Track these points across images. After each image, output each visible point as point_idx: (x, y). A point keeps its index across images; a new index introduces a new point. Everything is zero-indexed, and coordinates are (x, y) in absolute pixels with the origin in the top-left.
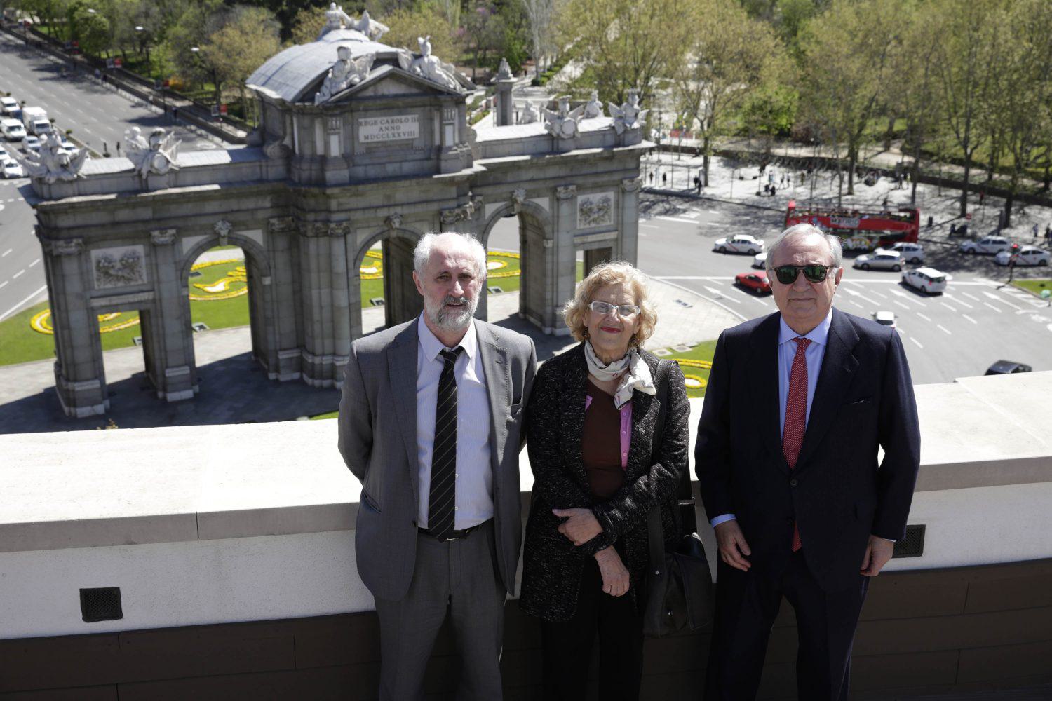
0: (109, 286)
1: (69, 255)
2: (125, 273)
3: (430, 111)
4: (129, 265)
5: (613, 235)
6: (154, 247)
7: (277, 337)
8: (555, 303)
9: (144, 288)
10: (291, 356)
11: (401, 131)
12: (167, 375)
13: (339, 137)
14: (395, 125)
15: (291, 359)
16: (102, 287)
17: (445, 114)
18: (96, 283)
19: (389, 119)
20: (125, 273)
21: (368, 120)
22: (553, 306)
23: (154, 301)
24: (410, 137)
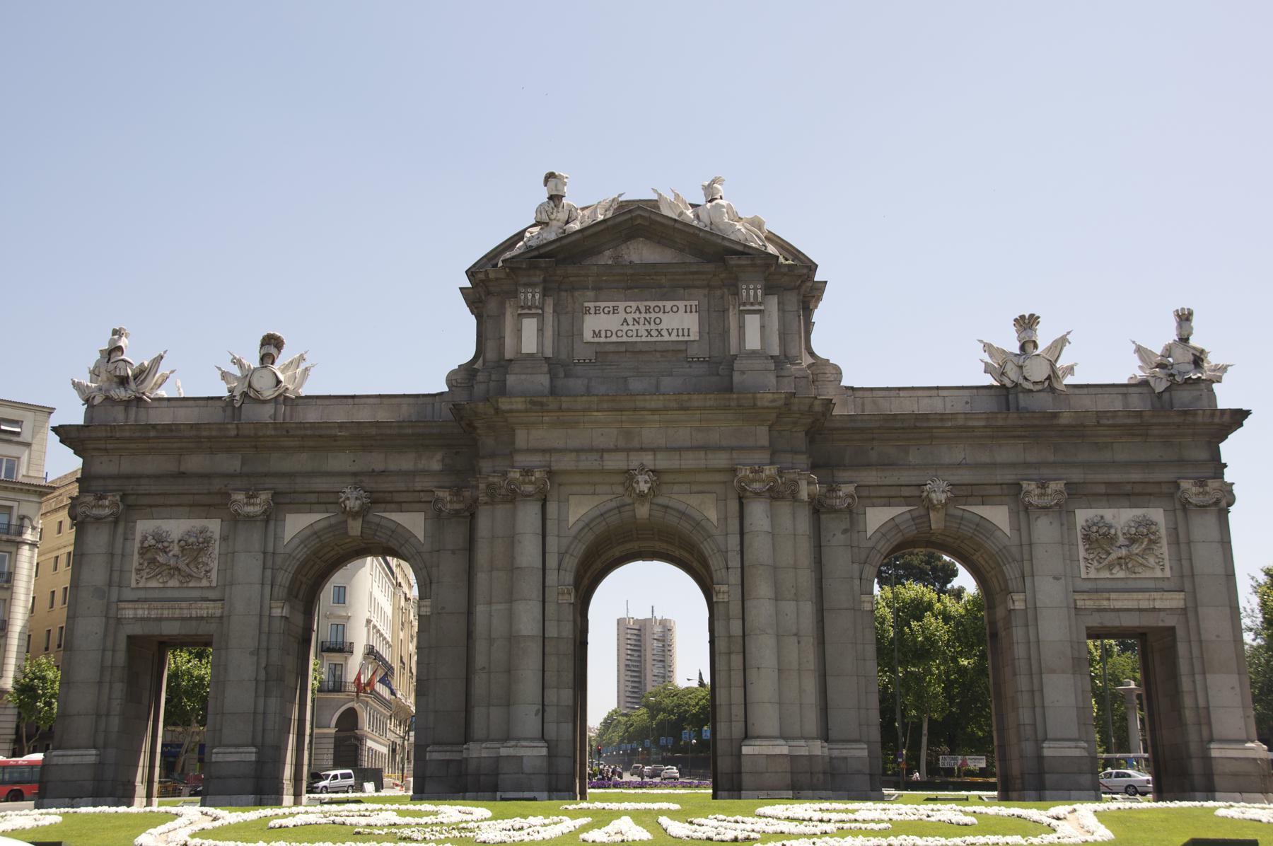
0: (153, 584)
1: (98, 519)
3: (722, 297)
5: (1175, 601)
6: (236, 521)
8: (1040, 735)
9: (211, 595)
10: (448, 756)
11: (663, 326)
14: (653, 315)
15: (448, 762)
16: (141, 585)
18: (134, 576)
19: (642, 305)
21: (602, 305)
22: (1036, 740)
23: (221, 617)
24: (681, 338)
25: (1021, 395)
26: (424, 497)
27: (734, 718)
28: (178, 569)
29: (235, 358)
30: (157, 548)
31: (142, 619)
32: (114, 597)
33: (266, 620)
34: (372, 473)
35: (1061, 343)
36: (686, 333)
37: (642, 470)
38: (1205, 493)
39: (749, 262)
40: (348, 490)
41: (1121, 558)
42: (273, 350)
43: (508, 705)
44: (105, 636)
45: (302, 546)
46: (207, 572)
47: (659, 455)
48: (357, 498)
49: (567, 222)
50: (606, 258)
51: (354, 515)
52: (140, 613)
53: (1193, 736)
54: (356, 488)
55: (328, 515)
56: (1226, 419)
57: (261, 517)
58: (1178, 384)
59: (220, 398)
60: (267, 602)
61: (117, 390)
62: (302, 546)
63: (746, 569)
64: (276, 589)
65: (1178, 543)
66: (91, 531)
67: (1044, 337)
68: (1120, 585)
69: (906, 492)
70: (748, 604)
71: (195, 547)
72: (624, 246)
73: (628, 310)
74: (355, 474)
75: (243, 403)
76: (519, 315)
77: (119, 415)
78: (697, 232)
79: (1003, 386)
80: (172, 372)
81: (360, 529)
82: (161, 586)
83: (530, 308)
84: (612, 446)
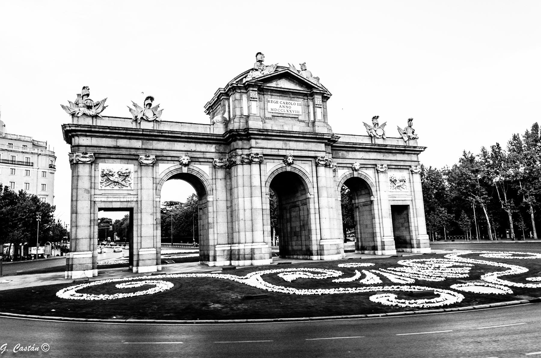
1: (84, 163)
2: (120, 180)
4: (125, 176)
6: (141, 165)
7: (216, 235)
8: (382, 235)
9: (131, 192)
12: (140, 253)
13: (257, 104)
14: (288, 105)
15: (224, 250)
16: (102, 189)
17: (317, 101)
18: (100, 185)
19: (285, 101)
20: (120, 180)
21: (273, 100)
22: (381, 237)
23: (137, 201)
24: (297, 114)
25: (376, 139)
26: (211, 160)
27: (317, 233)
28: (117, 182)
29: (134, 103)
30: (110, 175)
31: (104, 201)
32: (93, 193)
33: (155, 202)
34: (191, 151)
35: (384, 124)
36: (298, 112)
37: (290, 156)
38: (416, 169)
39: (319, 91)
40: (183, 156)
41: (398, 186)
42: (149, 101)
43: (253, 231)
44: (91, 208)
45: (166, 175)
46: (130, 184)
47: (295, 151)
48: (187, 159)
49: (262, 71)
50: (273, 84)
51: (186, 165)
52: (103, 199)
53: (414, 234)
54: (186, 156)
55: (175, 165)
56: (423, 150)
57: (151, 165)
58: (411, 139)
59: (131, 119)
60: (155, 195)
61: (89, 112)
62: (166, 175)
63: (319, 188)
64: (157, 190)
65: (410, 182)
66: (81, 167)
67: (380, 121)
68: (397, 193)
69: (348, 165)
70: (319, 198)
71: (125, 175)
72: (279, 81)
73: (281, 103)
74: (185, 151)
75: (141, 121)
76: (250, 100)
77: (88, 121)
78: (304, 80)
79: (370, 136)
80: (107, 106)
81: (187, 171)
82: (112, 189)
83: (254, 98)
84: (281, 148)
